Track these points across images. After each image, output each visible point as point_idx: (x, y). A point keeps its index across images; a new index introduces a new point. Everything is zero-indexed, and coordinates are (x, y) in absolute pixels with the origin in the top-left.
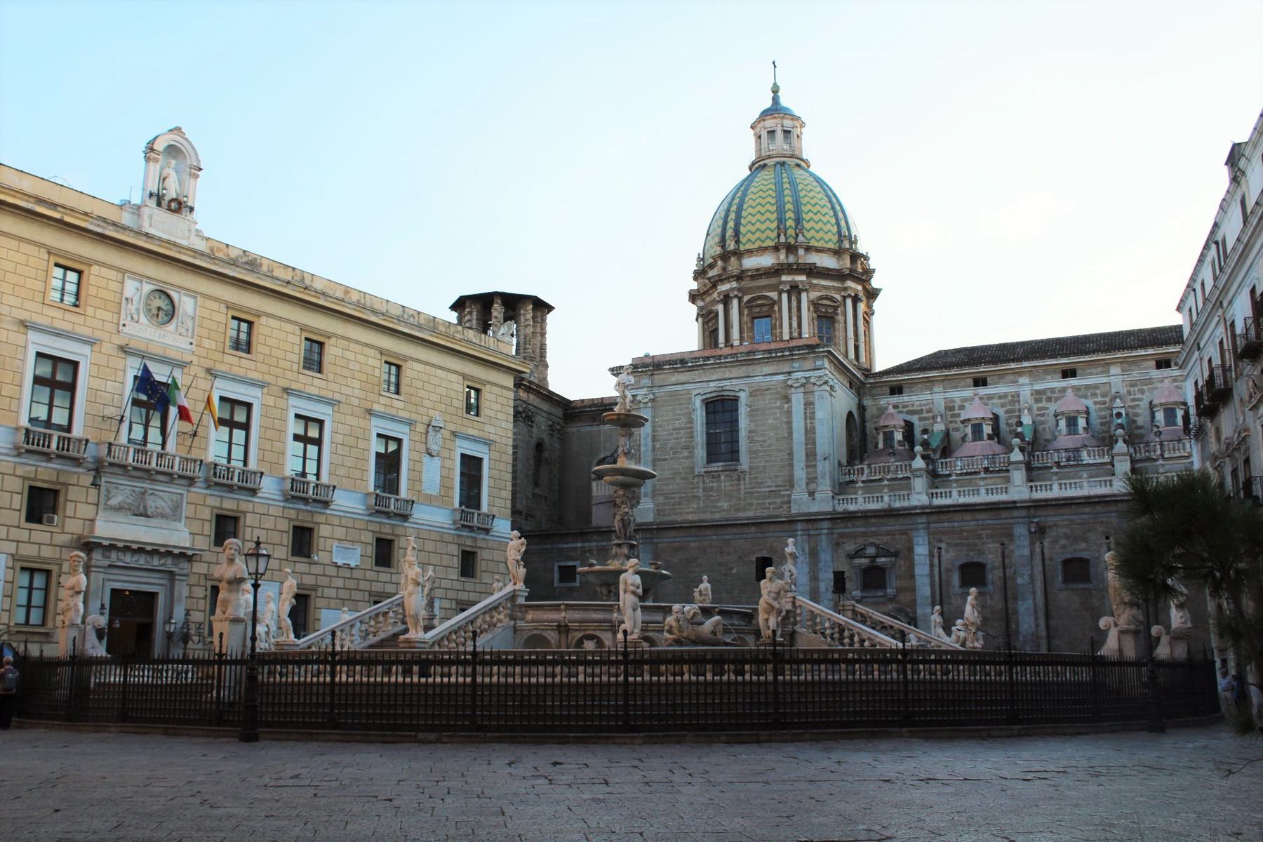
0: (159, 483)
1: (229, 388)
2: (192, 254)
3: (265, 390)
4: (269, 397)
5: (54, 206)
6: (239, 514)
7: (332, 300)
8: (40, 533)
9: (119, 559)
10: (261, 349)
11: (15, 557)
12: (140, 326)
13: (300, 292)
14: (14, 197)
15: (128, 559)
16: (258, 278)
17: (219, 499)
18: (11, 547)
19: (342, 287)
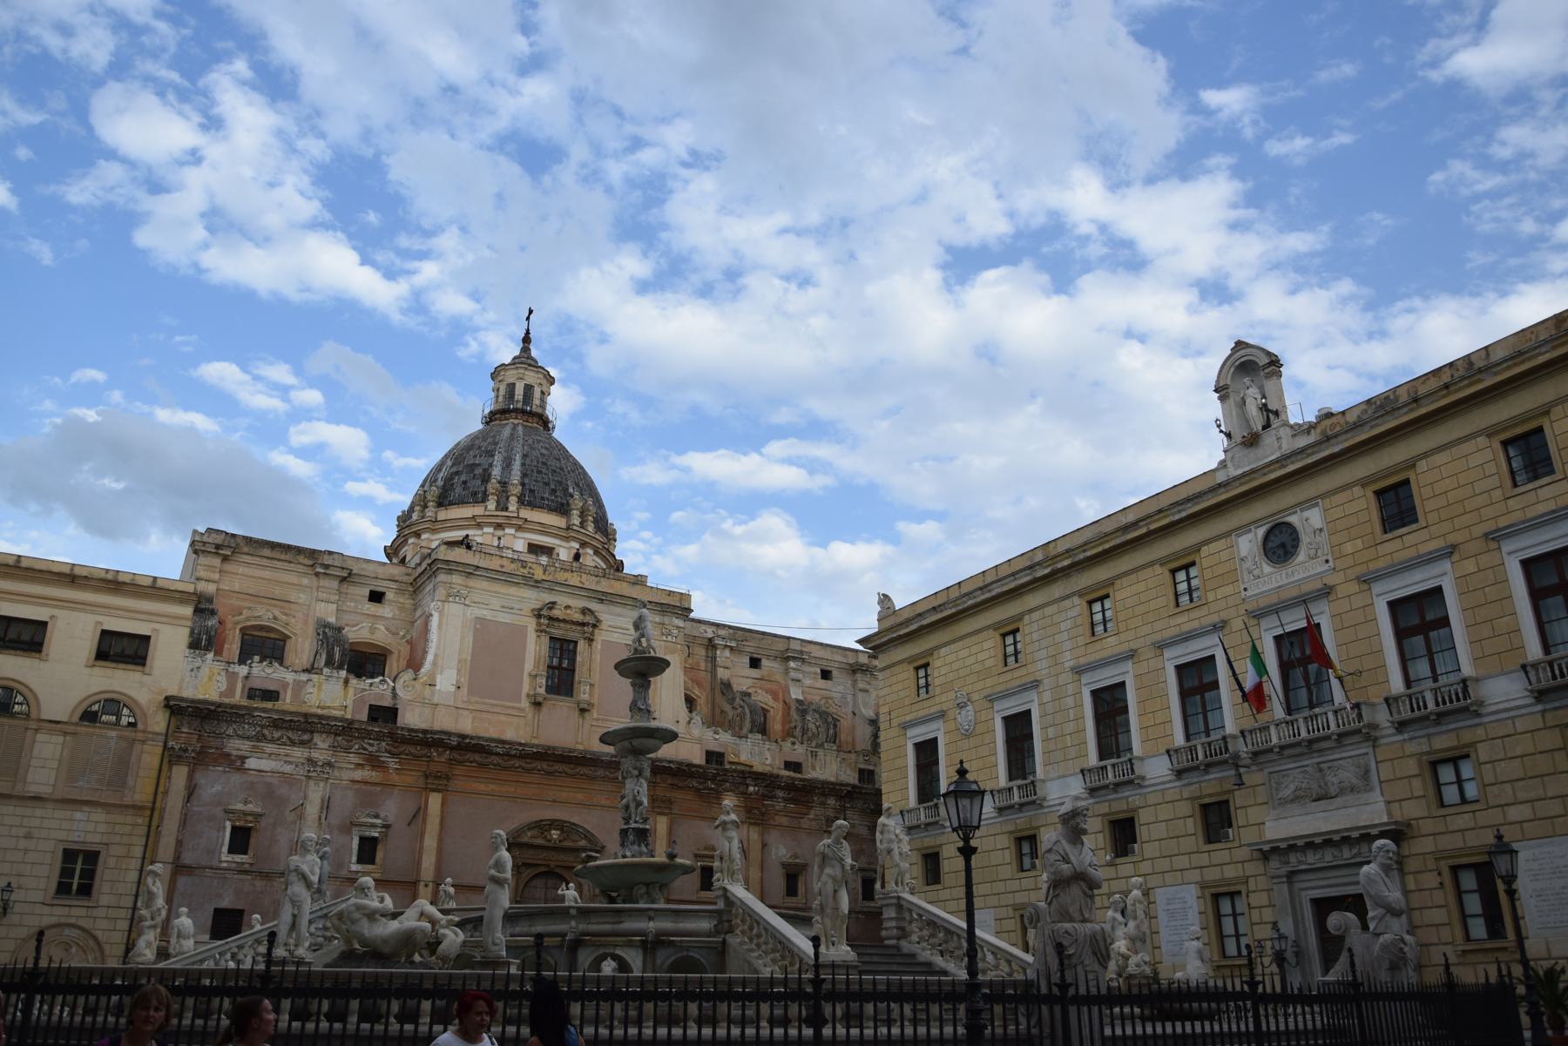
0: (1330, 752)
1: (1395, 586)
2: (1277, 465)
3: (1455, 557)
4: (1465, 562)
5: (1134, 525)
6: (1465, 750)
7: (1505, 365)
8: (1220, 853)
9: (1300, 862)
10: (1430, 505)
11: (1203, 886)
12: (1262, 580)
13: (1444, 396)
14: (1107, 541)
15: (1312, 858)
16: (1372, 427)
17: (1425, 739)
18: (1195, 875)
19: (1546, 325)
